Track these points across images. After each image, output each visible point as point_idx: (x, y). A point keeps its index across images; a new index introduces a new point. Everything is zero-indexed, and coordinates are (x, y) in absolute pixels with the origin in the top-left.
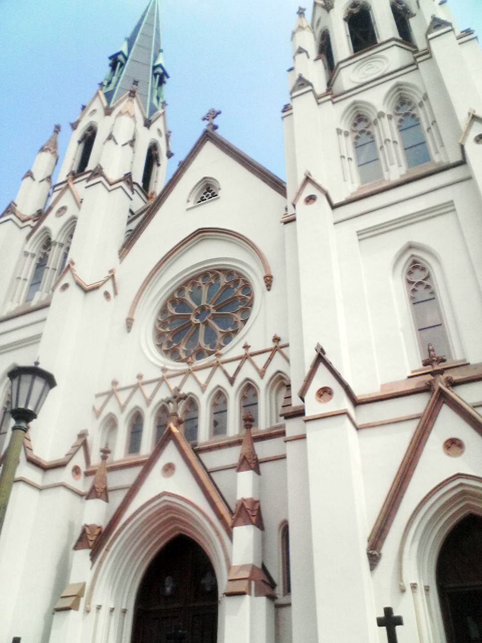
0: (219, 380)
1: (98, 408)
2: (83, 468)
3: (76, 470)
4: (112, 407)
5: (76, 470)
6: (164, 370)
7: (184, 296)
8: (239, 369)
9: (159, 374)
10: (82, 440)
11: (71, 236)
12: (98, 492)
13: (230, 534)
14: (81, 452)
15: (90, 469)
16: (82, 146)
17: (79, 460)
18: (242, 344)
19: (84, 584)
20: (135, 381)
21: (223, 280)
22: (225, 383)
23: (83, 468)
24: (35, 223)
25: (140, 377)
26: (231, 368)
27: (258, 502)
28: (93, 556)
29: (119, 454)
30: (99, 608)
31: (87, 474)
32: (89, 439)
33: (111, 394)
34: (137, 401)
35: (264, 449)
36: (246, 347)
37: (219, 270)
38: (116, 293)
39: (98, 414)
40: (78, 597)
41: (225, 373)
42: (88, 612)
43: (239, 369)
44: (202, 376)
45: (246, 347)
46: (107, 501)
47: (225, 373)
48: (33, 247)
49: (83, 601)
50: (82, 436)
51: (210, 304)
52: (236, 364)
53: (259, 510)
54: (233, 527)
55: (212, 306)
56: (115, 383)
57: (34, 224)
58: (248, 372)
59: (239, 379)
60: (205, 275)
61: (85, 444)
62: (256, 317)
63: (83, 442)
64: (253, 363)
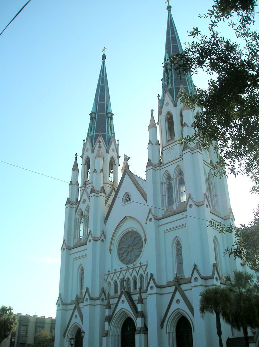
3: (103, 299)
4: (109, 279)
6: (121, 268)
9: (120, 270)
12: (109, 306)
14: (103, 294)
17: (103, 296)
18: (139, 262)
20: (114, 271)
23: (104, 298)
25: (115, 270)
28: (109, 323)
29: (112, 294)
31: (106, 299)
34: (115, 278)
35: (144, 296)
36: (140, 263)
37: (134, 231)
38: (105, 238)
41: (136, 271)
44: (131, 271)
45: (140, 263)
47: (136, 271)
48: (78, 215)
53: (143, 313)
54: (137, 318)
56: (109, 271)
58: (141, 272)
63: (103, 291)
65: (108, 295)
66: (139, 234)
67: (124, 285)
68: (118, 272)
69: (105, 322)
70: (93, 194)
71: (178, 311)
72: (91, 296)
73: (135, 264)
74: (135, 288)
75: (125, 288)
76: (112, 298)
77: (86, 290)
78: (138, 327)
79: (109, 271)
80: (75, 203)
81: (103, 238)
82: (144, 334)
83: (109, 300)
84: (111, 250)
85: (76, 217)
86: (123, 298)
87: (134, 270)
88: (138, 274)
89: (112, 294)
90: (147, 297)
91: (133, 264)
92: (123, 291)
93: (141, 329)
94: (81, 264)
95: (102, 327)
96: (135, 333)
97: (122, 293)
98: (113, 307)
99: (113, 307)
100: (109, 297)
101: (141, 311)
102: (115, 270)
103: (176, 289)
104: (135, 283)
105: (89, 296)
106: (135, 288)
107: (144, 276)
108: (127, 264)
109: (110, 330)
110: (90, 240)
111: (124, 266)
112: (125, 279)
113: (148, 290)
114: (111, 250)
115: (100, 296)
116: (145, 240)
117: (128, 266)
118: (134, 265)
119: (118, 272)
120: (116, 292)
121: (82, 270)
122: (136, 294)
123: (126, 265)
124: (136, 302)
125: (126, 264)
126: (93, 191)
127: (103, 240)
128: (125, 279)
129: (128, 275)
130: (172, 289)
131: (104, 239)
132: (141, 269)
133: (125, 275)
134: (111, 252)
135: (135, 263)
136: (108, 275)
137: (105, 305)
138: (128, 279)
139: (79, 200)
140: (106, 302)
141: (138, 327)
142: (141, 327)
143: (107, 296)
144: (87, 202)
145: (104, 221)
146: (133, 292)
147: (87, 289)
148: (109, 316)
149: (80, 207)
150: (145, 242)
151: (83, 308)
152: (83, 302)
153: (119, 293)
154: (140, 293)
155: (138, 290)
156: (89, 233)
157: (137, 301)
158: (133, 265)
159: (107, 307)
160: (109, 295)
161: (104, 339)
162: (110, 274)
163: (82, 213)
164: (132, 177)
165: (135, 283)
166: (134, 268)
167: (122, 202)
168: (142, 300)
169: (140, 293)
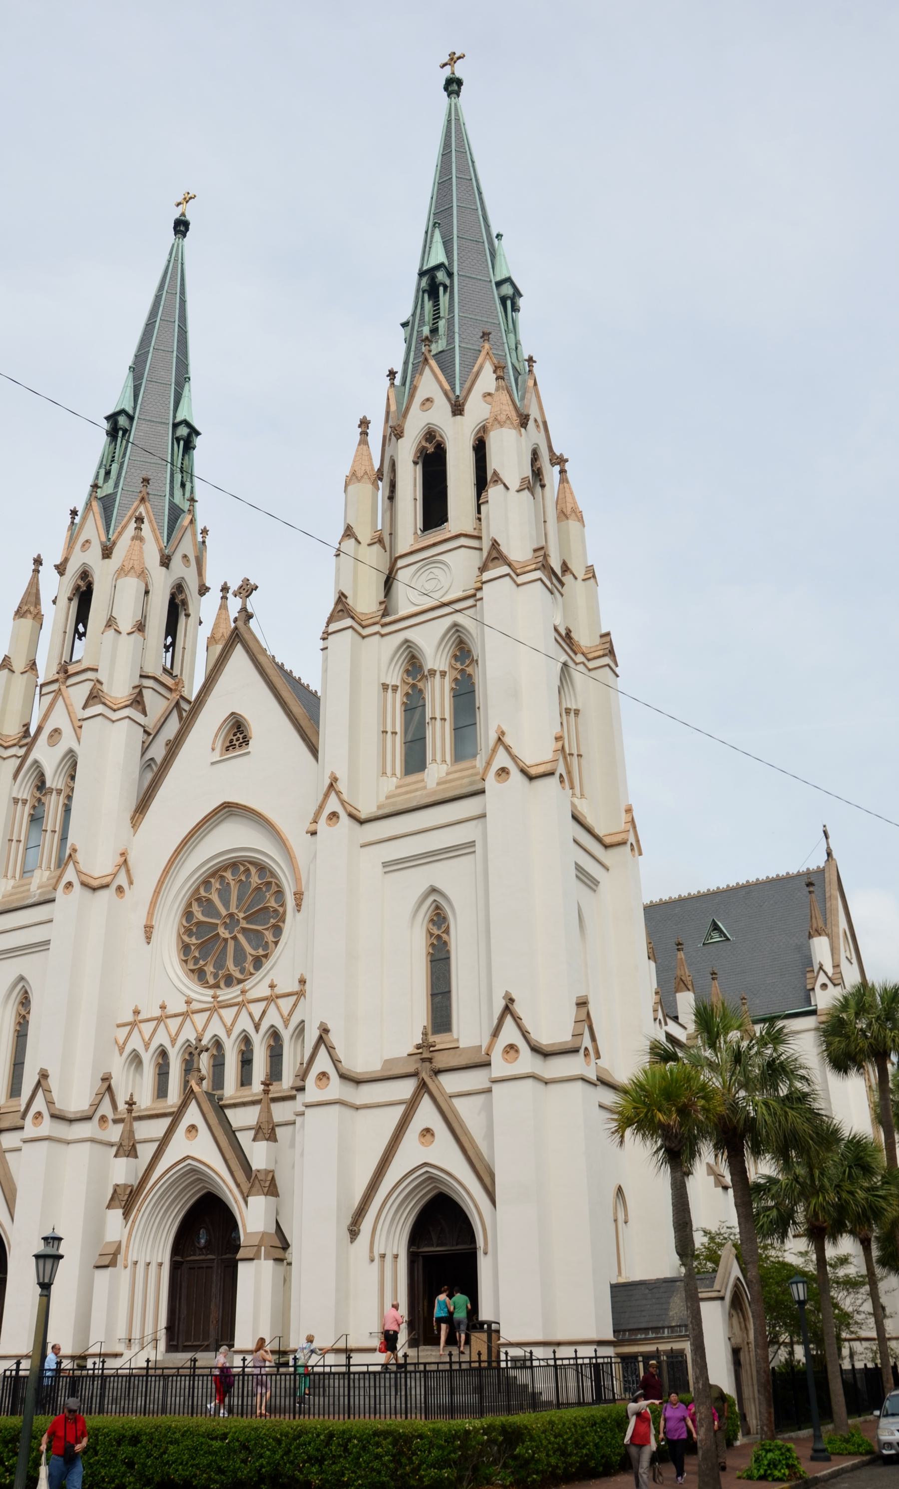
0: (245, 1023)
1: (121, 1042)
2: (110, 1115)
4: (135, 1043)
5: (103, 1118)
6: (188, 1002)
7: (211, 894)
8: (264, 1013)
9: (183, 1008)
10: (106, 1085)
11: (73, 778)
13: (246, 1203)
14: (107, 1099)
15: (118, 1117)
16: (75, 604)
17: (106, 1108)
18: (267, 982)
19: (120, 1242)
20: (157, 1013)
21: (255, 880)
22: (251, 1030)
23: (110, 1115)
24: (24, 750)
26: (257, 1009)
27: (273, 1171)
28: (126, 1215)
29: (145, 1100)
30: (136, 1263)
31: (115, 1121)
32: (113, 1082)
33: (133, 1024)
34: (161, 1038)
35: (281, 1112)
36: (272, 986)
38: (131, 883)
39: (121, 1050)
40: (115, 1254)
41: (251, 1015)
42: (126, 1267)
43: (264, 1013)
44: (228, 1014)
45: (272, 986)
46: (136, 1157)
47: (251, 1015)
48: (25, 790)
49: (120, 1258)
50: (106, 1079)
51: (239, 912)
52: (262, 1005)
53: (273, 1178)
54: (248, 1196)
55: (241, 915)
56: (137, 1012)
57: (22, 752)
58: (273, 1018)
59: (264, 1026)
60: (233, 865)
61: (109, 1088)
62: (286, 943)
64: (278, 1008)
65: (127, 1103)
66: (273, 874)
67: (201, 1067)
68: (176, 1016)
69: (109, 1207)
70: (98, 709)
71: (427, 1172)
72: (57, 1105)
73: (247, 988)
74: (245, 1080)
75: (202, 1079)
76: (140, 1118)
77: (36, 1078)
78: (248, 1231)
79: (137, 1012)
80: (15, 742)
81: (122, 879)
82: (276, 1260)
83: (131, 1125)
84: (149, 930)
85: (14, 795)
86: (193, 1115)
87: (244, 1013)
88: (257, 1027)
89: (145, 1100)
90: (299, 1120)
91: (241, 986)
92: (196, 1088)
93: (262, 1239)
94: (22, 978)
95: (96, 1228)
96: (239, 1256)
97: (188, 1095)
98: (146, 1152)
99: (146, 1152)
100: (130, 1111)
101: (267, 1172)
102: (163, 1007)
103: (423, 1087)
104: (246, 1062)
105: (50, 1103)
106: (245, 1080)
107: (286, 1035)
108: (217, 986)
109: (127, 1247)
110: (69, 884)
111: (203, 996)
112: (204, 1042)
113: (302, 1089)
114: (149, 930)
115: (96, 1106)
116: (299, 896)
117: (219, 992)
118: (243, 992)
119: (176, 1016)
120: (162, 1091)
121: (25, 1001)
122: (244, 1104)
123: (211, 992)
124: (245, 1139)
125: (210, 987)
126: (94, 697)
127: (120, 889)
128: (204, 1042)
129: (216, 1029)
130: (407, 1088)
131: (125, 885)
132: (272, 1008)
133: (204, 1030)
134: (148, 939)
135: (247, 985)
136: (133, 1024)
137: (112, 1145)
138: (218, 1044)
139: (32, 731)
140: (115, 1133)
141: (248, 1231)
142: (264, 1234)
143: (122, 1106)
144: (67, 741)
145: (133, 818)
146: (231, 1098)
147: (44, 1075)
148: (126, 1186)
149: (35, 754)
150: (298, 906)
151: (19, 1150)
152: (22, 1128)
153: (174, 1096)
154: (269, 1099)
155: (257, 1087)
156: (70, 856)
157: (252, 1133)
158: (239, 992)
159: (121, 1151)
160: (131, 1104)
161: (102, 1276)
162: (141, 1022)
163: (43, 782)
164: (261, 659)
165: (246, 1062)
166: (241, 1005)
167: (213, 749)
168: (273, 1129)
169: (269, 1099)
